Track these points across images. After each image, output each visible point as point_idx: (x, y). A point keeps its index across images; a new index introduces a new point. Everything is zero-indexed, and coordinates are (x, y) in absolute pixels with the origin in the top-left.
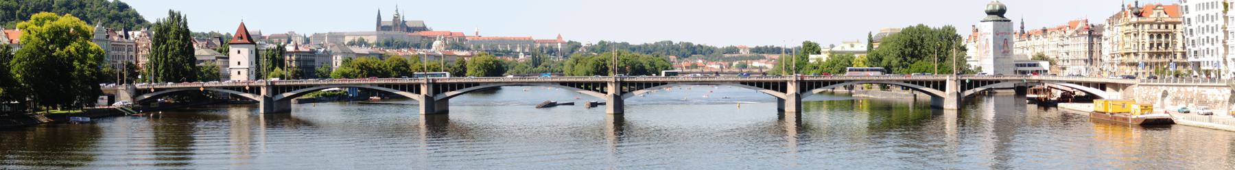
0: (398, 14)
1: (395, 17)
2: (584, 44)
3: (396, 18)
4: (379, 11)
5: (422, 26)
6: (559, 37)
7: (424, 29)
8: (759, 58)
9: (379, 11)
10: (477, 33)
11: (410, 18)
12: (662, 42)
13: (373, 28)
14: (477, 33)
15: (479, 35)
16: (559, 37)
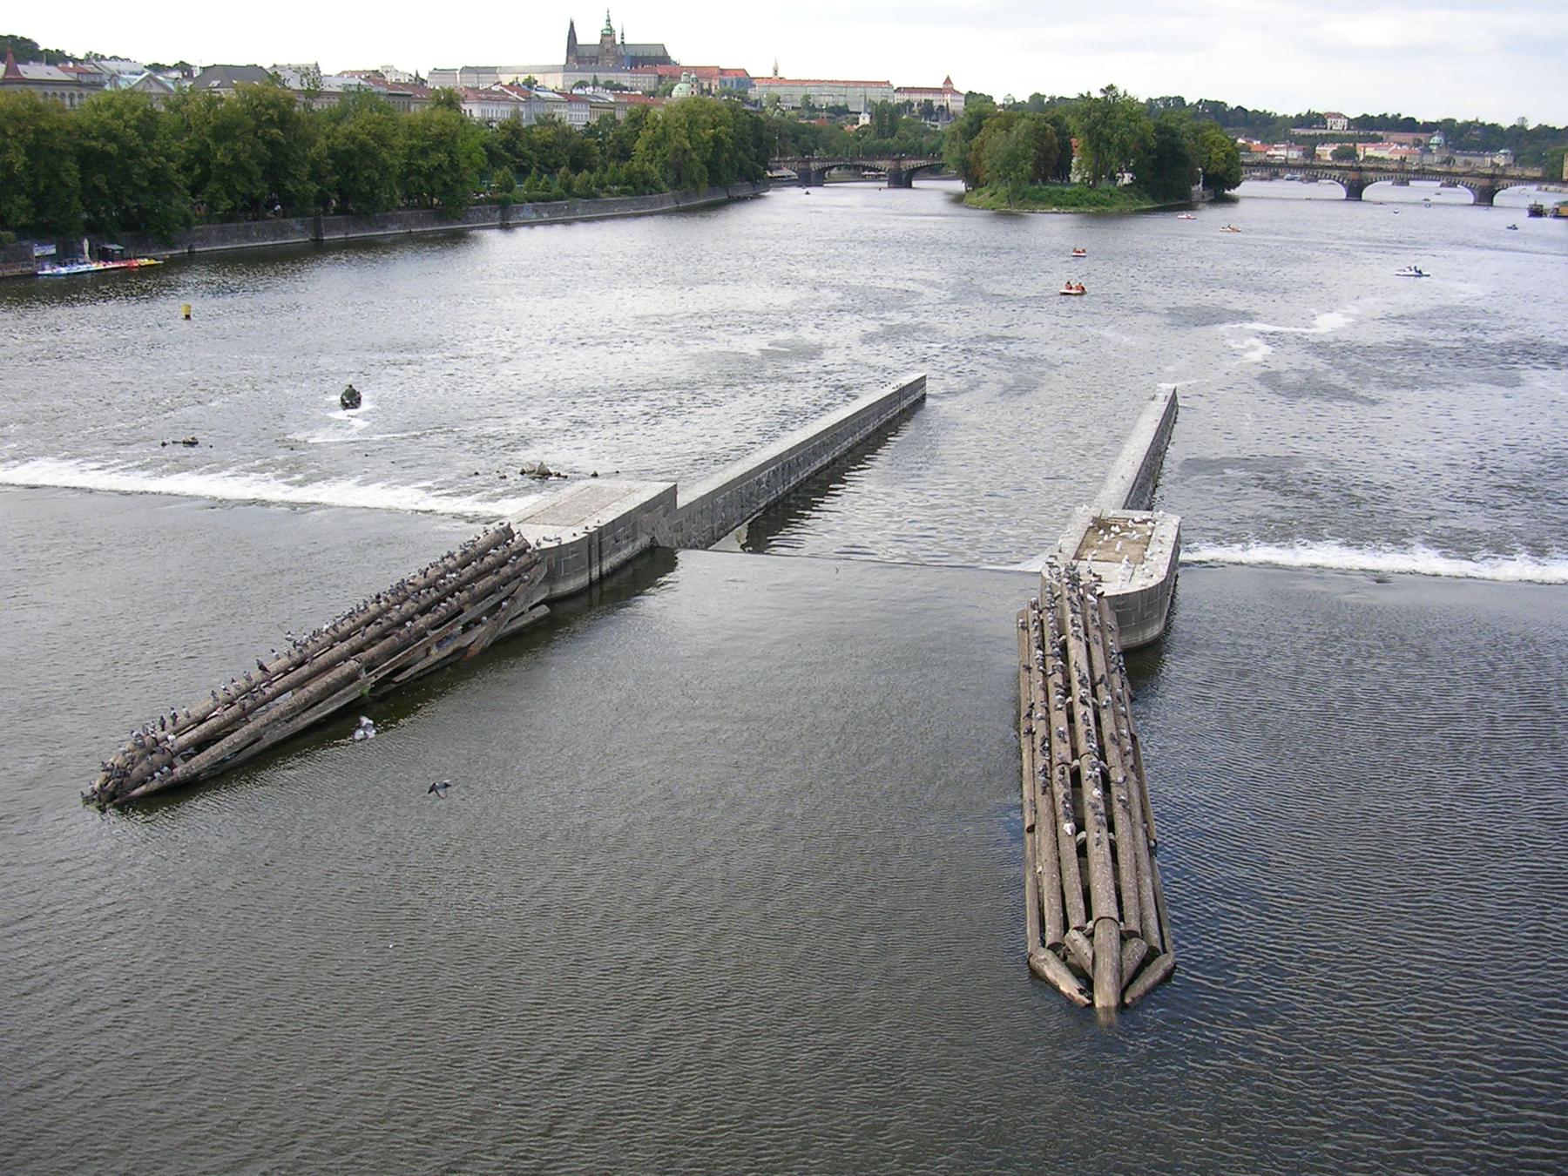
0: (611, 29)
1: (603, 35)
2: (999, 100)
3: (608, 34)
4: (572, 24)
5: (660, 54)
6: (948, 81)
7: (664, 59)
8: (1375, 140)
9: (572, 24)
10: (776, 72)
11: (636, 34)
12: (1162, 98)
13: (560, 57)
14: (776, 72)
15: (780, 75)
16: (948, 81)
